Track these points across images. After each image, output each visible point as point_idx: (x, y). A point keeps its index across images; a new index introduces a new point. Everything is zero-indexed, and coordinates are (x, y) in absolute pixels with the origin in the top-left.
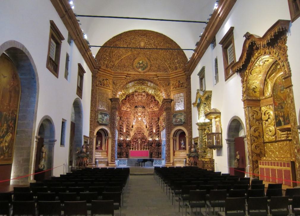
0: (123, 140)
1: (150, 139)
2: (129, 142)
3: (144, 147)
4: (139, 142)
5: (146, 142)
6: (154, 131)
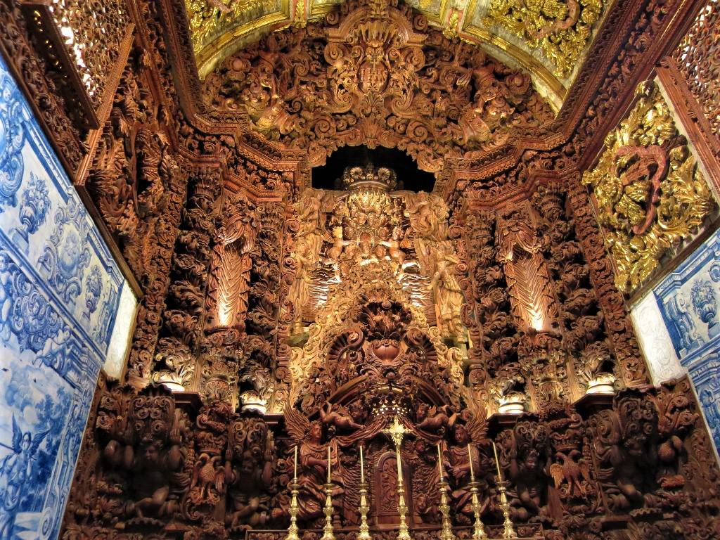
0: (191, 404)
1: (511, 406)
2: (260, 437)
3: (457, 508)
4: (397, 430)
5: (469, 440)
6: (536, 319)
